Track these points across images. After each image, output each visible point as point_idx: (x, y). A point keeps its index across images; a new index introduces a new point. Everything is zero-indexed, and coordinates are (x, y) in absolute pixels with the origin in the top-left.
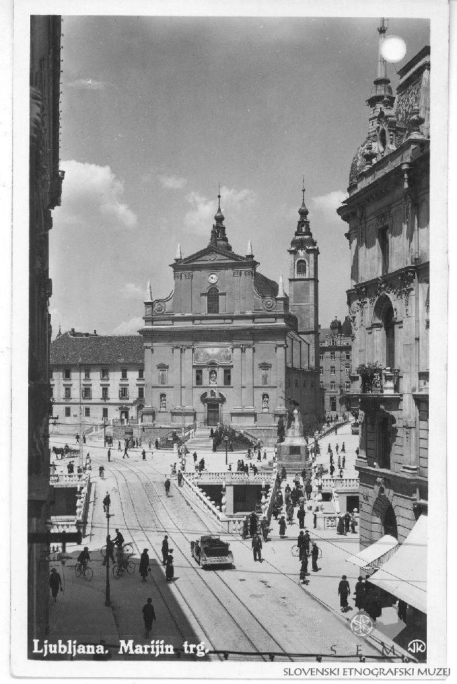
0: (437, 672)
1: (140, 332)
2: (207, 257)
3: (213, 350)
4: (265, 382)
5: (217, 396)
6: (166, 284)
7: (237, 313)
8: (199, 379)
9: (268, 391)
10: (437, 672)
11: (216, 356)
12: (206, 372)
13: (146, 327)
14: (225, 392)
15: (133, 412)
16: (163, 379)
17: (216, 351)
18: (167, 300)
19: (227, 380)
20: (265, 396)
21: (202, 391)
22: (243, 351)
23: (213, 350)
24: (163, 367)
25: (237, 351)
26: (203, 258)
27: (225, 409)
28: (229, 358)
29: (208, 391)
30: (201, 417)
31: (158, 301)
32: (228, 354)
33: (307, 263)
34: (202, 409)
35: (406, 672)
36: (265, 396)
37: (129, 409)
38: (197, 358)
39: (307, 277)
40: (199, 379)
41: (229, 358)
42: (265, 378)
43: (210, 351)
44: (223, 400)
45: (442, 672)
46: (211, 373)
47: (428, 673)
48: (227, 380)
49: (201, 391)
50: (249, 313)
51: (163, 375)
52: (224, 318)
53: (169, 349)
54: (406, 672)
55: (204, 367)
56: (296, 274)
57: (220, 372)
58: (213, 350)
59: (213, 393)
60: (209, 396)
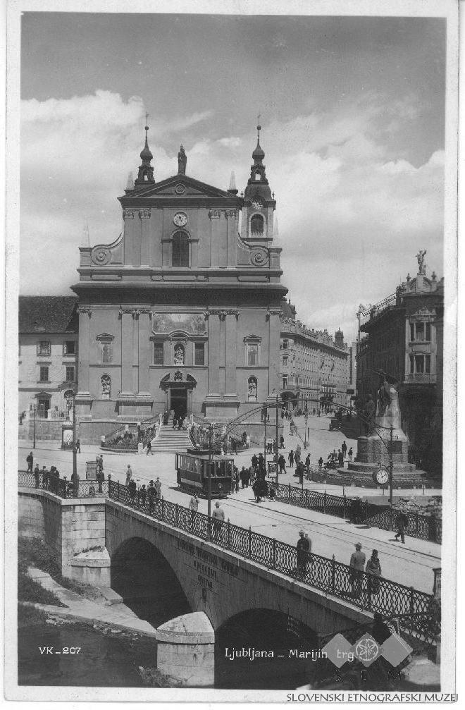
0: (444, 698)
1: (74, 288)
2: (172, 189)
3: (179, 318)
4: (252, 362)
5: (184, 380)
6: (109, 227)
7: (214, 268)
8: (159, 359)
9: (256, 374)
10: (444, 698)
11: (187, 325)
12: (169, 347)
13: (81, 282)
14: (197, 375)
15: (58, 400)
16: (106, 354)
17: (183, 318)
18: (110, 246)
19: (200, 359)
20: (253, 379)
21: (163, 373)
22: (223, 318)
23: (179, 318)
24: (106, 338)
25: (214, 319)
26: (166, 191)
27: (196, 398)
28: (202, 328)
29: (172, 373)
30: (160, 410)
31: (100, 247)
32: (201, 323)
33: (265, 220)
34: (164, 397)
35: (413, 698)
36: (253, 379)
37: (51, 396)
38: (156, 327)
39: (264, 236)
40: (159, 359)
41: (202, 328)
42: (252, 355)
43: (174, 318)
44: (192, 383)
45: (449, 698)
46: (176, 348)
47: (435, 699)
48: (200, 359)
49: (163, 373)
50: (230, 268)
51: (105, 349)
52: (197, 274)
53: (115, 314)
54: (413, 698)
55: (166, 338)
56: (250, 232)
57: (191, 348)
58: (179, 318)
59: (178, 376)
60: (171, 380)
